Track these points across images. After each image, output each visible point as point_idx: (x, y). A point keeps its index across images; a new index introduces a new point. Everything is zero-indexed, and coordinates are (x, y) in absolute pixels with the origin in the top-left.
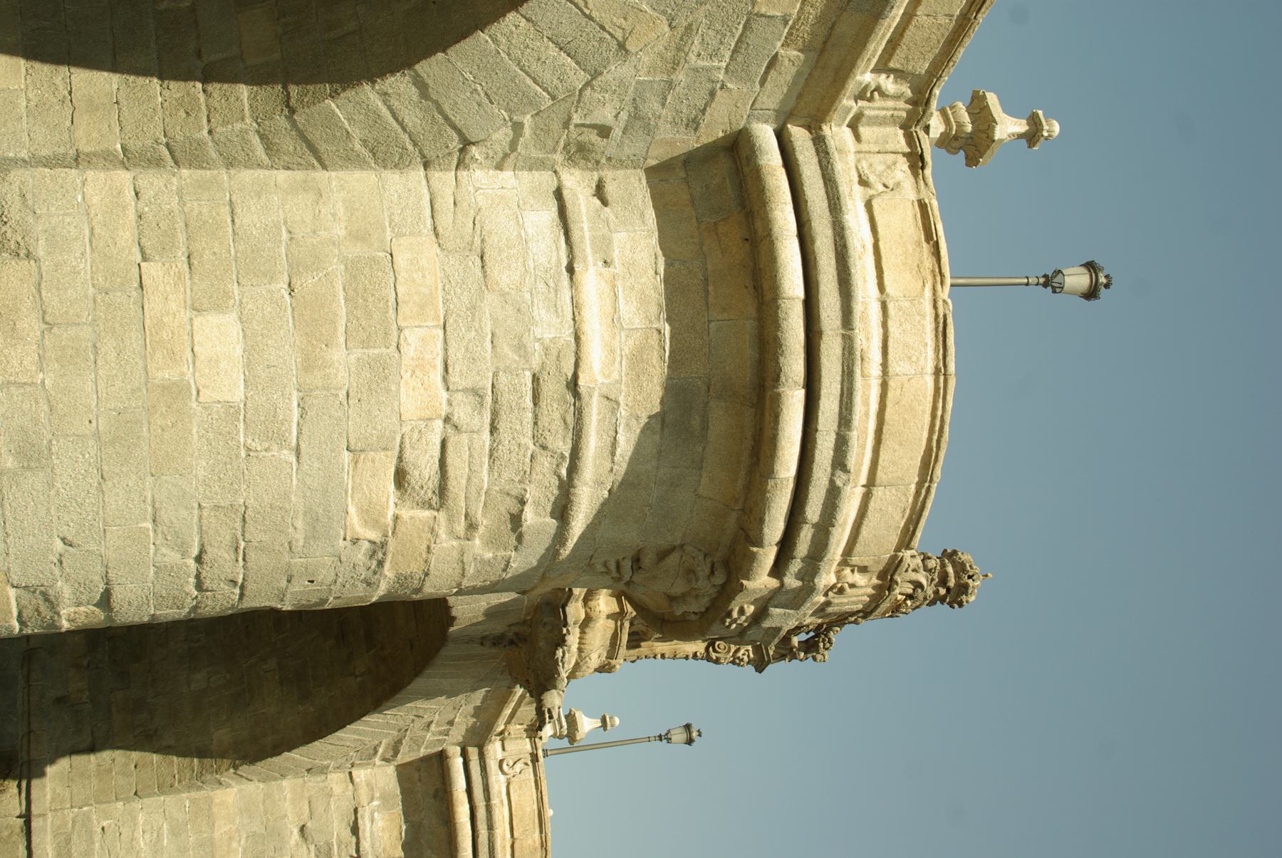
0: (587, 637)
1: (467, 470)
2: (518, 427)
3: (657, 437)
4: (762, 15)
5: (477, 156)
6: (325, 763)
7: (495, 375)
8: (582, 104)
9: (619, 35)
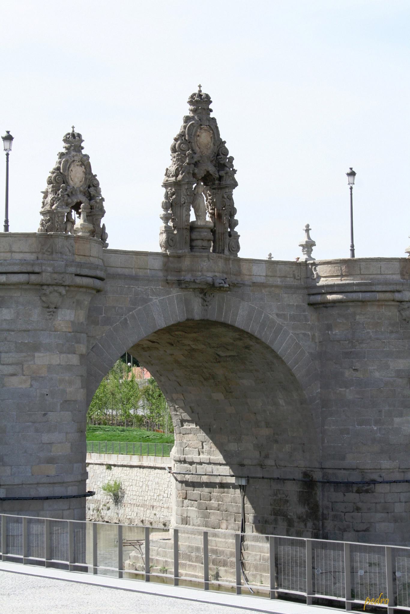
3: (3, 309)
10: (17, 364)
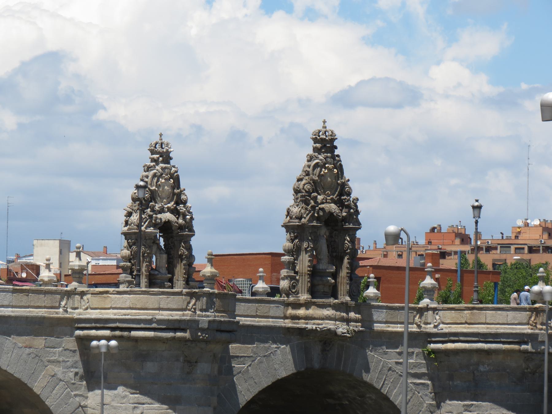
0: (316, 317)
1: (154, 410)
4: (45, 345)
5: (83, 403)
6: (425, 405)
7: (130, 403)
8: (69, 381)
9: (50, 377)
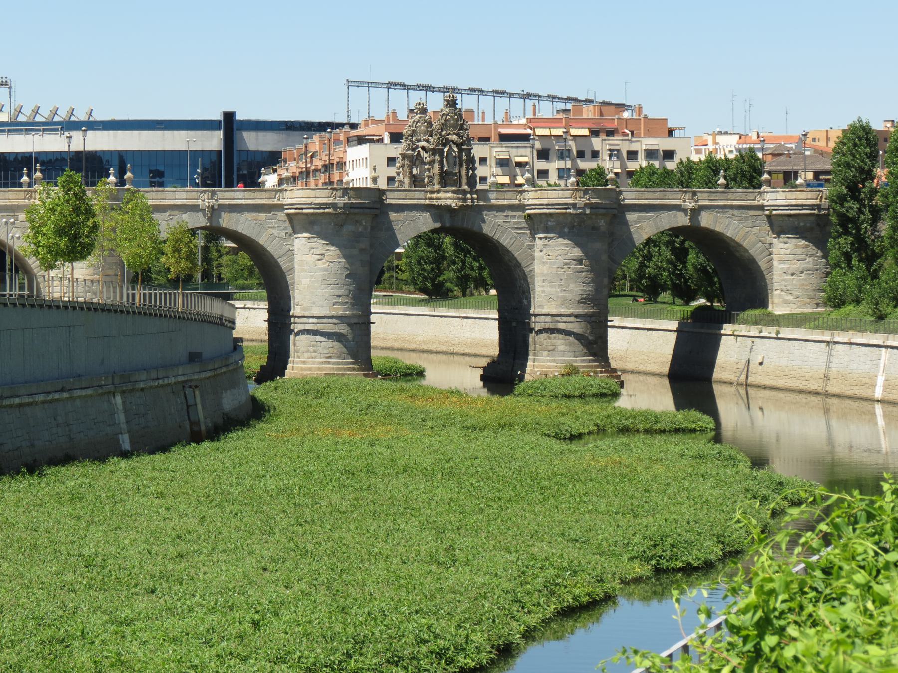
2: (313, 245)
10: (321, 255)
